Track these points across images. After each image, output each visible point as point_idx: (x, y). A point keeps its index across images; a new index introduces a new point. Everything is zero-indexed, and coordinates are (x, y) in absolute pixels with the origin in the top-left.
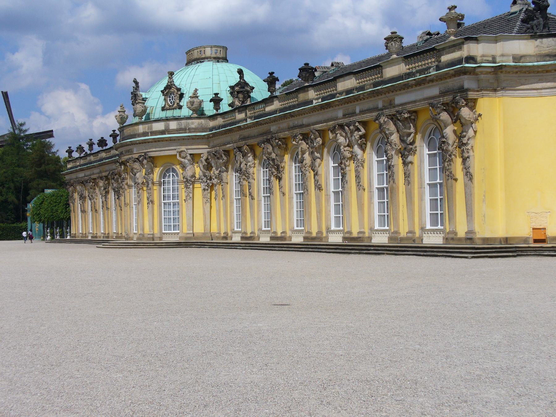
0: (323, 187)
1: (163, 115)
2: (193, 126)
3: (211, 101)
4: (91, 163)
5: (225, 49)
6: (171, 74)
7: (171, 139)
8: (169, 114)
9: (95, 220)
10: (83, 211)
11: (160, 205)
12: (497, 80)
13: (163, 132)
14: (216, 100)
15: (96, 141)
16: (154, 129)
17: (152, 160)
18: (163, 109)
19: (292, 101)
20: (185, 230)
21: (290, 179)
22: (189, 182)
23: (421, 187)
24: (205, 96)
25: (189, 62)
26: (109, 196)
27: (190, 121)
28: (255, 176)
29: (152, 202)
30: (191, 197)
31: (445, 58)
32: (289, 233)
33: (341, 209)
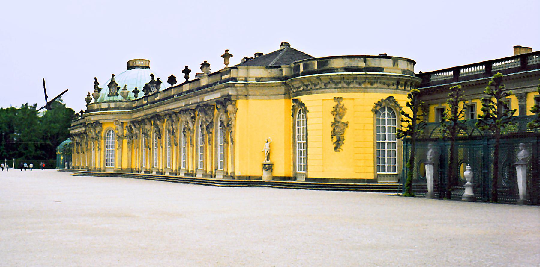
0: (178, 144)
1: (108, 99)
2: (123, 106)
3: (133, 92)
6: (113, 76)
7: (110, 114)
11: (105, 152)
12: (247, 90)
13: (106, 109)
14: (136, 92)
16: (102, 107)
18: (109, 96)
20: (117, 166)
23: (216, 147)
24: (130, 89)
28: (152, 136)
30: (121, 147)
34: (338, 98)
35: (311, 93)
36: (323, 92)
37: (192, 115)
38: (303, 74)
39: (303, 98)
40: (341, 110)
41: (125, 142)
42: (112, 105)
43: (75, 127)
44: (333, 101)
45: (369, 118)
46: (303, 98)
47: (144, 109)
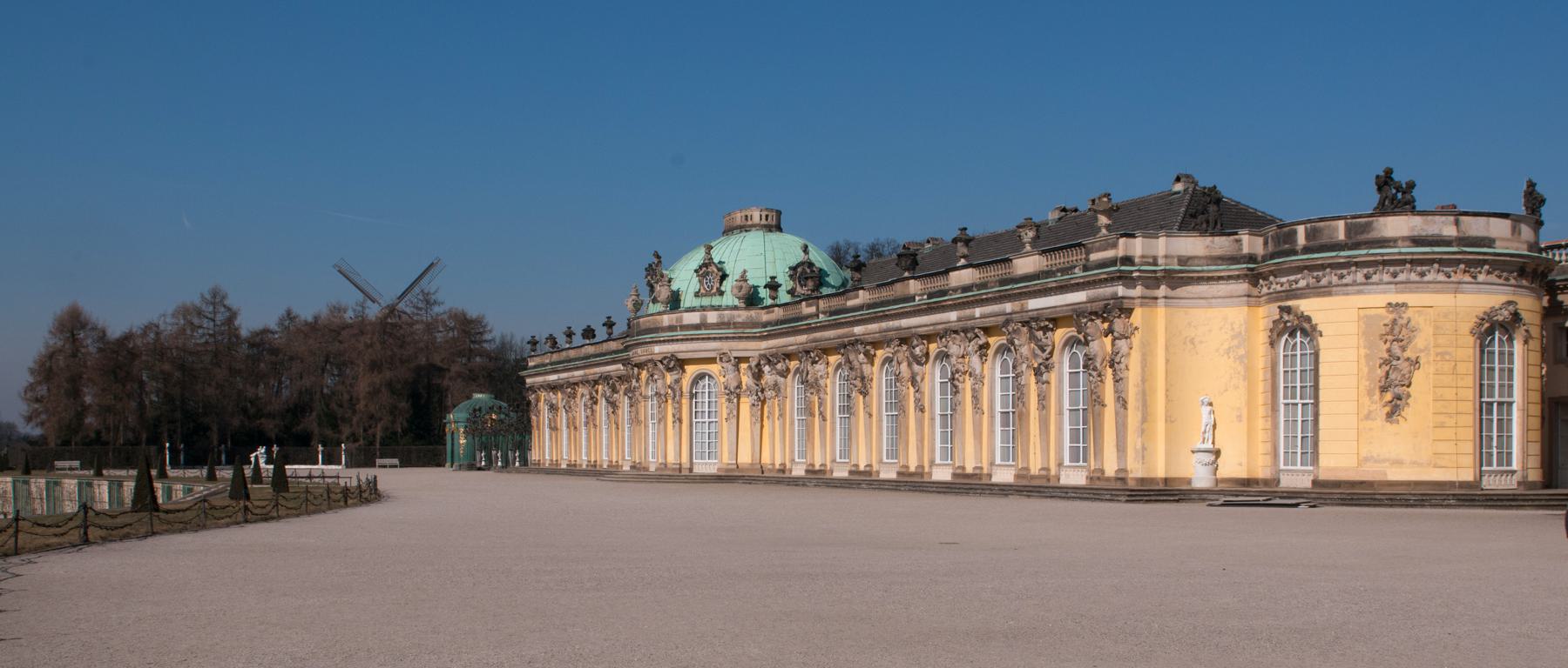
1: (696, 302)
4: (570, 361)
5: (779, 213)
6: (710, 248)
8: (706, 301)
9: (574, 441)
10: (554, 428)
13: (696, 327)
15: (578, 331)
16: (685, 322)
17: (680, 364)
18: (697, 295)
19: (885, 294)
20: (726, 459)
21: (880, 395)
22: (735, 393)
23: (1060, 413)
24: (758, 279)
25: (729, 231)
26: (597, 408)
27: (735, 313)
28: (829, 390)
29: (680, 421)
31: (1094, 257)
32: (875, 468)
33: (951, 434)
34: (1397, 305)
35: (1329, 294)
36: (1359, 292)
37: (982, 341)
38: (1306, 250)
39: (1305, 305)
40: (1404, 331)
41: (746, 403)
42: (712, 317)
43: (542, 370)
44: (1383, 311)
45: (1467, 349)
46: (1305, 305)
47: (810, 329)
